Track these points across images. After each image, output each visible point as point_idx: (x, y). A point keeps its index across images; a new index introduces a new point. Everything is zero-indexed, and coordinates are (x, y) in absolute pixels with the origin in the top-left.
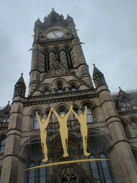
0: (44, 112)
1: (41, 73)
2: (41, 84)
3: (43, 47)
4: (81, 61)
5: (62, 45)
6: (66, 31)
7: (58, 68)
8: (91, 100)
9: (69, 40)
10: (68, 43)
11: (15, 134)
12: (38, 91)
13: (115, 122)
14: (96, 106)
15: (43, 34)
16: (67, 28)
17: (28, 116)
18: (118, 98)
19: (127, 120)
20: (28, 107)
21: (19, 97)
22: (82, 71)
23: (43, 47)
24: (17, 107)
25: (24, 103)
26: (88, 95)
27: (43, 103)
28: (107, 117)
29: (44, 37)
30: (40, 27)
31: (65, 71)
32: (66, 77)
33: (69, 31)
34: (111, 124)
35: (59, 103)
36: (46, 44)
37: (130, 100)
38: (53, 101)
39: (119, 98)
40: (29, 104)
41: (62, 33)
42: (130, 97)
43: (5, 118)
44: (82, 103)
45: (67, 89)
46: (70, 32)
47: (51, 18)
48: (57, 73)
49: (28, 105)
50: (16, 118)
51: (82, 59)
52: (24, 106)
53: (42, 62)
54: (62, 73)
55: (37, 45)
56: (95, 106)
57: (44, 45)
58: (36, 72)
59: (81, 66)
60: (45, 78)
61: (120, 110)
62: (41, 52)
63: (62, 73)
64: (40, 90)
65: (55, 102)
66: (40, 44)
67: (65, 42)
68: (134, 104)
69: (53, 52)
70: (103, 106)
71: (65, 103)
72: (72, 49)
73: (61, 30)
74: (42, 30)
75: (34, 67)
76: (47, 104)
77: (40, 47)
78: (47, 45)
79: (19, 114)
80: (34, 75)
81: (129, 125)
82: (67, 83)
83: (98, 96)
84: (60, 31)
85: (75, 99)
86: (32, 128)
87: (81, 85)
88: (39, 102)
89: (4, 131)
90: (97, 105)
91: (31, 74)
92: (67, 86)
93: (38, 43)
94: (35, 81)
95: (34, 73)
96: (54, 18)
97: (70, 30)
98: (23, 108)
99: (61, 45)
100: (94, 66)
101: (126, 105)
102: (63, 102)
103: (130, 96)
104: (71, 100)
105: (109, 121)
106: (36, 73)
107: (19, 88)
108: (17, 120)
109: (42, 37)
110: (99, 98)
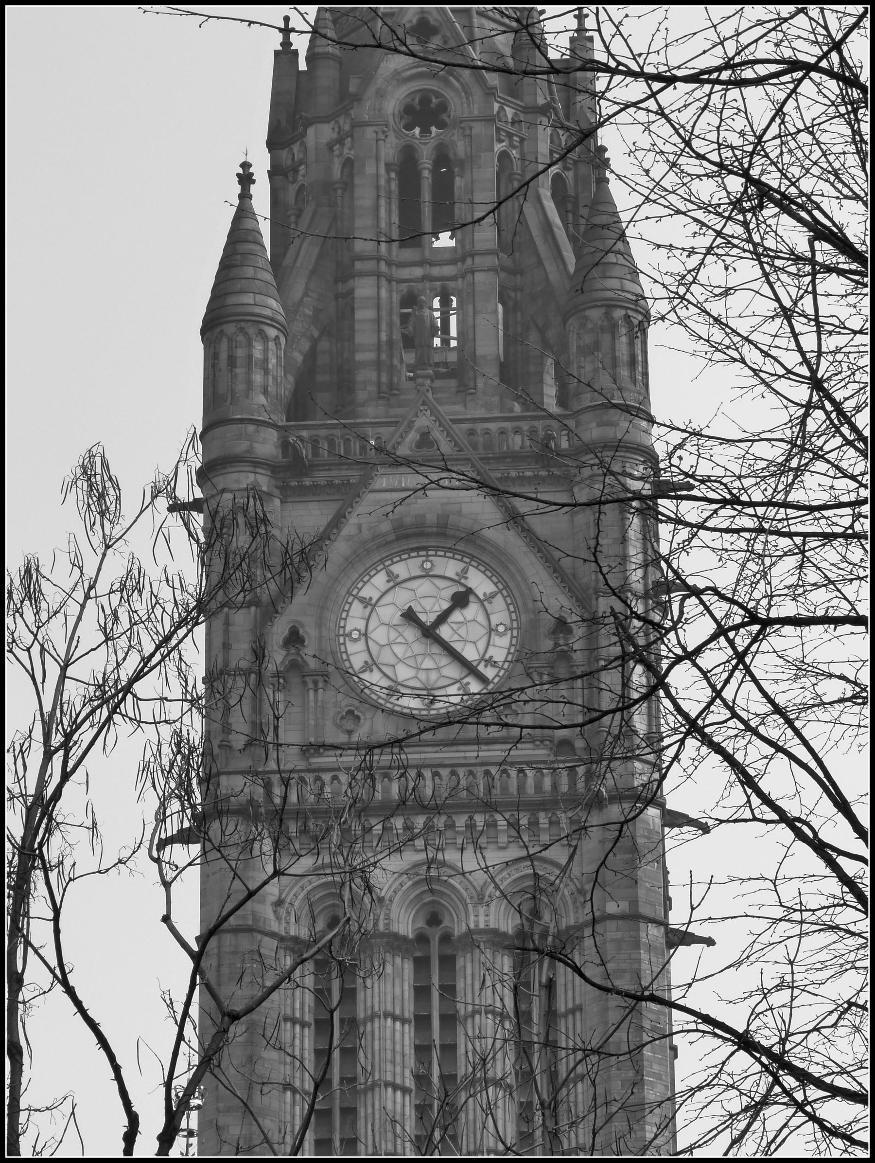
30: (274, 469)
47: (389, 150)
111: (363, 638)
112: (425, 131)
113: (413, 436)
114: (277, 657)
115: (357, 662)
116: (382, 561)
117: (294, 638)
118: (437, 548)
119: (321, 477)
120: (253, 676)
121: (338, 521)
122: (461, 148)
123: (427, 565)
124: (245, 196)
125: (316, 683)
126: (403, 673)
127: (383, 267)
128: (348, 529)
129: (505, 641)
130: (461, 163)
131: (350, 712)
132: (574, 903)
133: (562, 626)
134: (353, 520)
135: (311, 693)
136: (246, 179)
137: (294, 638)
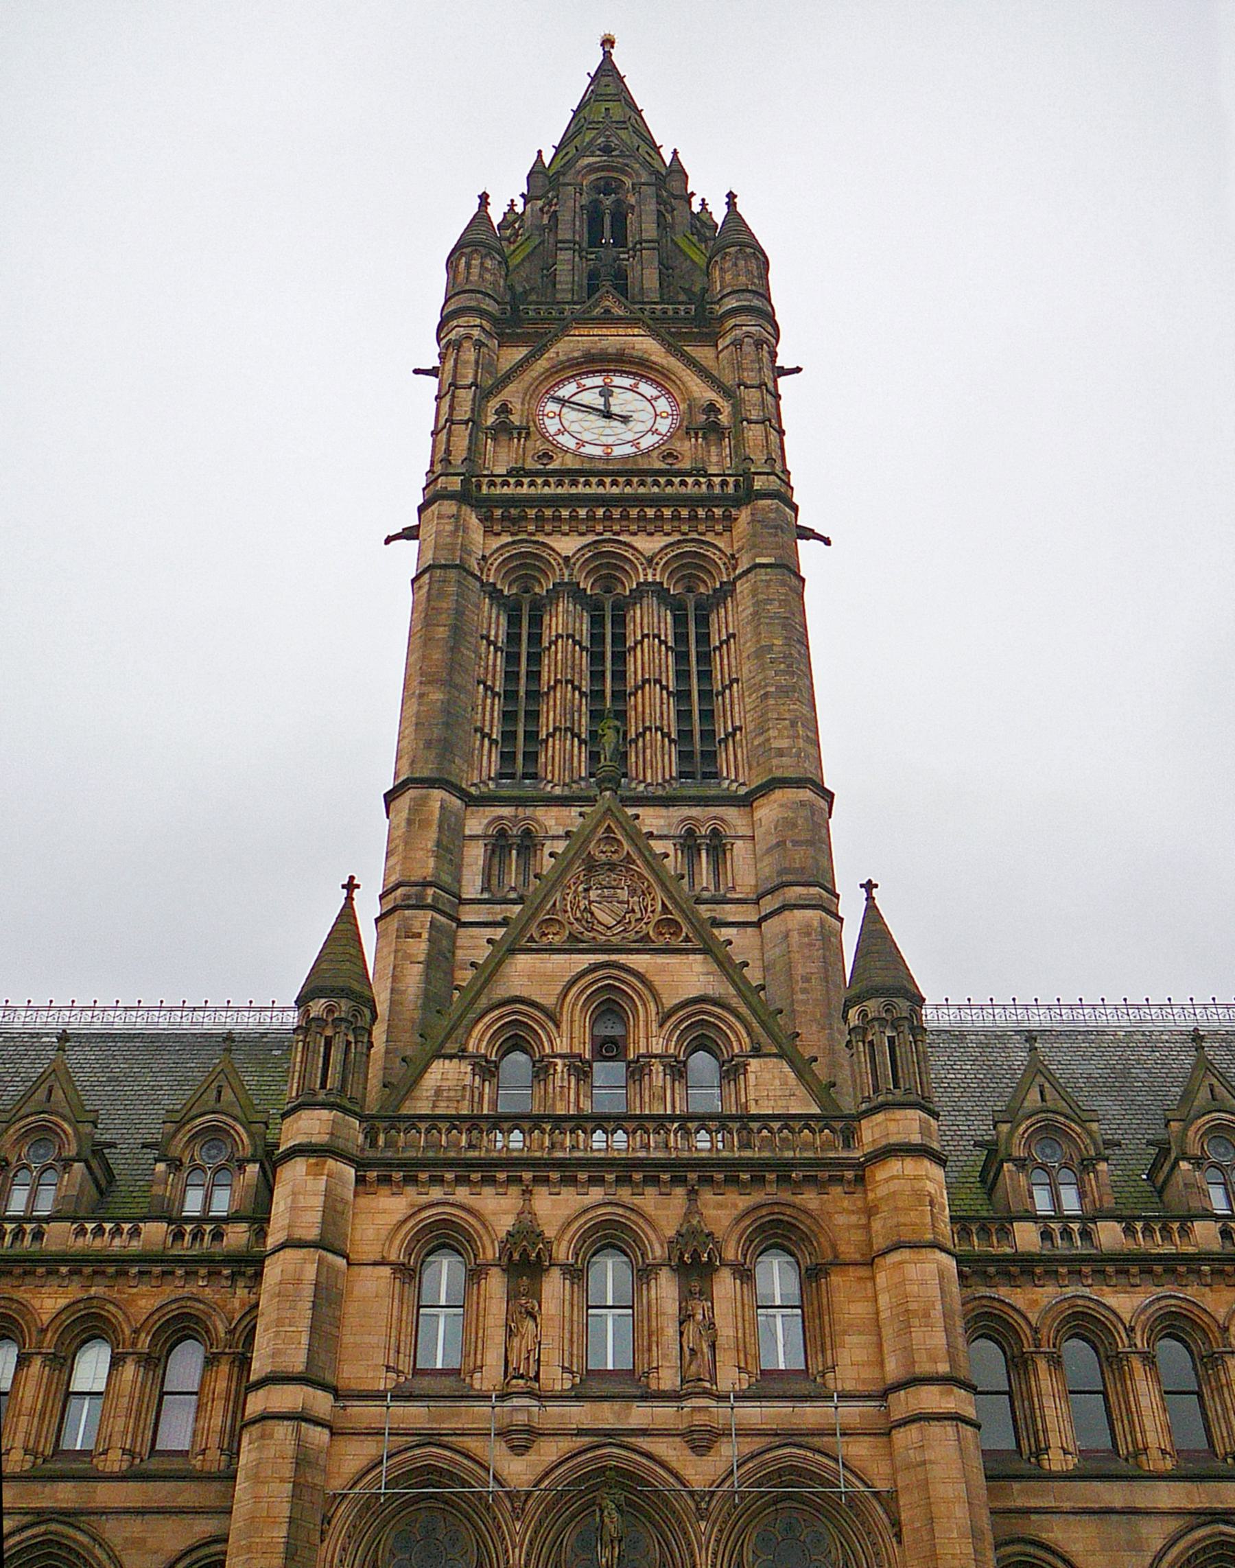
0: (491, 1252)
1: (472, 801)
2: (483, 1002)
3: (507, 539)
4: (784, 743)
5: (659, 542)
6: (704, 393)
7: (612, 867)
8: (810, 1199)
9: (707, 501)
10: (702, 528)
11: (301, 1417)
12: (461, 1055)
13: (935, 1429)
14: (840, 1264)
15: (512, 394)
16: (704, 354)
17: (386, 1271)
18: (1005, 1128)
19: (1036, 1331)
20: (385, 1190)
21: (325, 1114)
22: (781, 844)
23: (507, 539)
24: (319, 1201)
25: (360, 1164)
26: (790, 1164)
27: (489, 1181)
28: (893, 1369)
29: (520, 428)
31: (659, 907)
32: (661, 959)
33: (721, 403)
34: (913, 1431)
35: (596, 1194)
36: (532, 513)
37: (1087, 1165)
38: (555, 1176)
39: (1012, 1132)
40: (397, 1176)
41: (663, 405)
42: (1090, 1133)
43: (196, 1178)
44: (747, 1213)
45: (657, 1067)
46: (724, 419)
47: (584, 200)
48: (597, 912)
49: (385, 1180)
50: (308, 1291)
51: (793, 724)
52: (360, 1180)
53: (486, 688)
54: (633, 917)
55: (456, 517)
56: (830, 1258)
57: (514, 521)
58: (438, 794)
59: (780, 795)
60: (512, 951)
61: (1006, 1233)
62: (483, 584)
63: (639, 916)
64: (471, 1048)
65: (571, 1181)
66: (484, 506)
67: (676, 517)
68: (1109, 1203)
69: (576, 593)
70: (881, 1279)
71: (637, 1200)
72: (726, 592)
74: (506, 340)
75: (428, 744)
76: (514, 1190)
78: (532, 528)
79: (330, 1256)
80: (425, 824)
81: (1042, 1365)
82: (661, 1026)
83: (860, 1180)
85: (707, 1181)
86: (405, 1365)
87: (757, 1052)
88: (462, 1172)
89: (191, 1289)
90: (849, 1251)
91: (404, 802)
92: (657, 1048)
93: (464, 497)
94: (426, 884)
95: (418, 807)
96: (608, 201)
97: (727, 393)
98: (356, 1194)
99: (648, 544)
100: (870, 898)
101: (1056, 1199)
102: (624, 1194)
103: (1094, 1126)
104: (678, 1180)
105: (903, 1403)
106: (437, 814)
107: (329, 1032)
108: (314, 1306)
109: (503, 429)
110: (865, 1191)
111: (557, 417)
113: (597, 311)
115: (552, 430)
116: (572, 377)
117: (504, 409)
118: (615, 371)
120: (471, 424)
121: (543, 350)
122: (632, 200)
123: (608, 381)
125: (519, 434)
126: (586, 437)
127: (577, 247)
128: (551, 353)
129: (669, 421)
130: (632, 207)
131: (545, 454)
132: (727, 569)
133: (712, 408)
135: (516, 440)
137: (504, 409)
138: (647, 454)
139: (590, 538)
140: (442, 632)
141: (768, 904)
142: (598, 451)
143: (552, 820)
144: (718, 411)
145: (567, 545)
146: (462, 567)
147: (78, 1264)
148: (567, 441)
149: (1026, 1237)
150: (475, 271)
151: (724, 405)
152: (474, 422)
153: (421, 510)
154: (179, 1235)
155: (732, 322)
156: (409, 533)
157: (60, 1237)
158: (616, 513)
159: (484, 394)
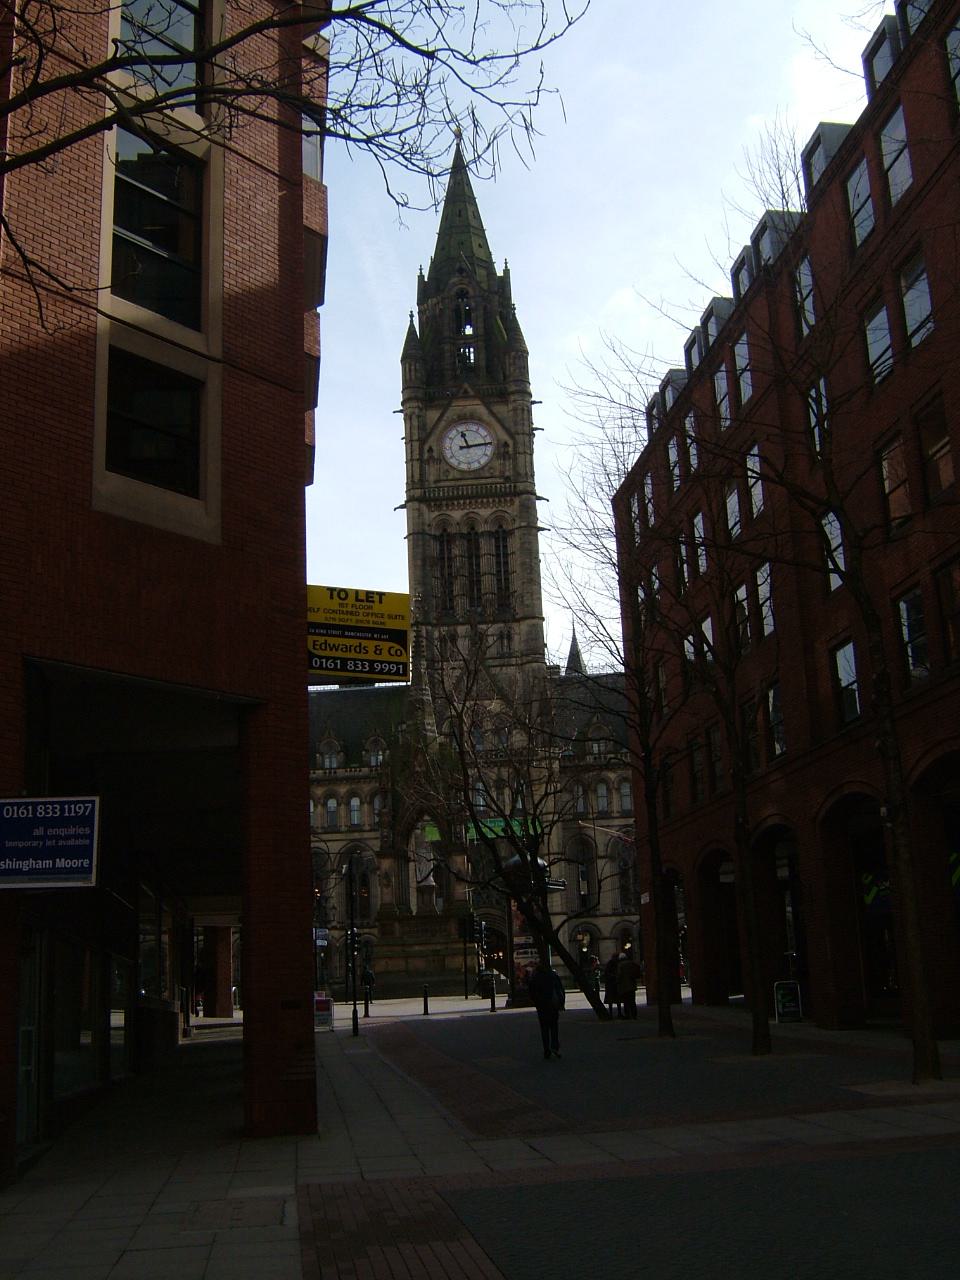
3: (437, 513)
6: (505, 437)
9: (505, 495)
15: (432, 442)
16: (500, 409)
23: (437, 513)
33: (510, 442)
36: (444, 503)
46: (511, 449)
59: (528, 621)
61: (584, 758)
72: (511, 532)
73: (487, 424)
77: (431, 516)
84: (486, 429)
93: (421, 500)
97: (512, 435)
99: (485, 512)
112: (463, 300)
113: (462, 391)
114: (426, 456)
117: (430, 450)
119: (436, 403)
121: (442, 415)
124: (412, 321)
133: (506, 445)
134: (446, 415)
136: (412, 316)
138: (482, 468)
139: (466, 511)
140: (419, 563)
141: (525, 659)
142: (464, 467)
143: (461, 630)
144: (508, 446)
145: (457, 515)
146: (423, 533)
147: (348, 780)
148: (453, 462)
149: (590, 759)
150: (413, 377)
151: (510, 442)
152: (421, 460)
153: (406, 502)
154: (371, 771)
155: (512, 398)
156: (402, 507)
157: (341, 773)
158: (473, 501)
159: (422, 441)
